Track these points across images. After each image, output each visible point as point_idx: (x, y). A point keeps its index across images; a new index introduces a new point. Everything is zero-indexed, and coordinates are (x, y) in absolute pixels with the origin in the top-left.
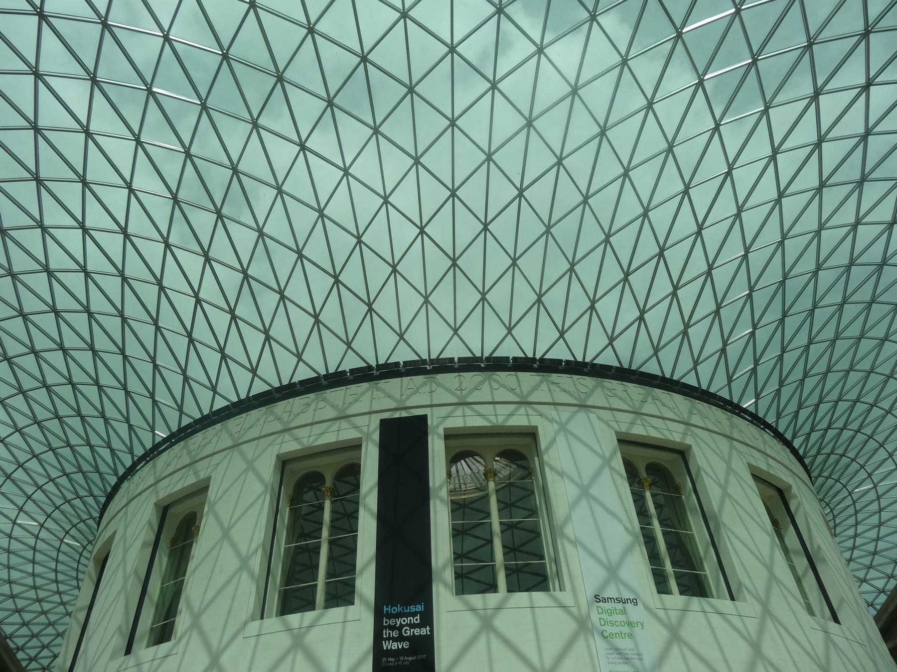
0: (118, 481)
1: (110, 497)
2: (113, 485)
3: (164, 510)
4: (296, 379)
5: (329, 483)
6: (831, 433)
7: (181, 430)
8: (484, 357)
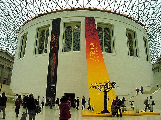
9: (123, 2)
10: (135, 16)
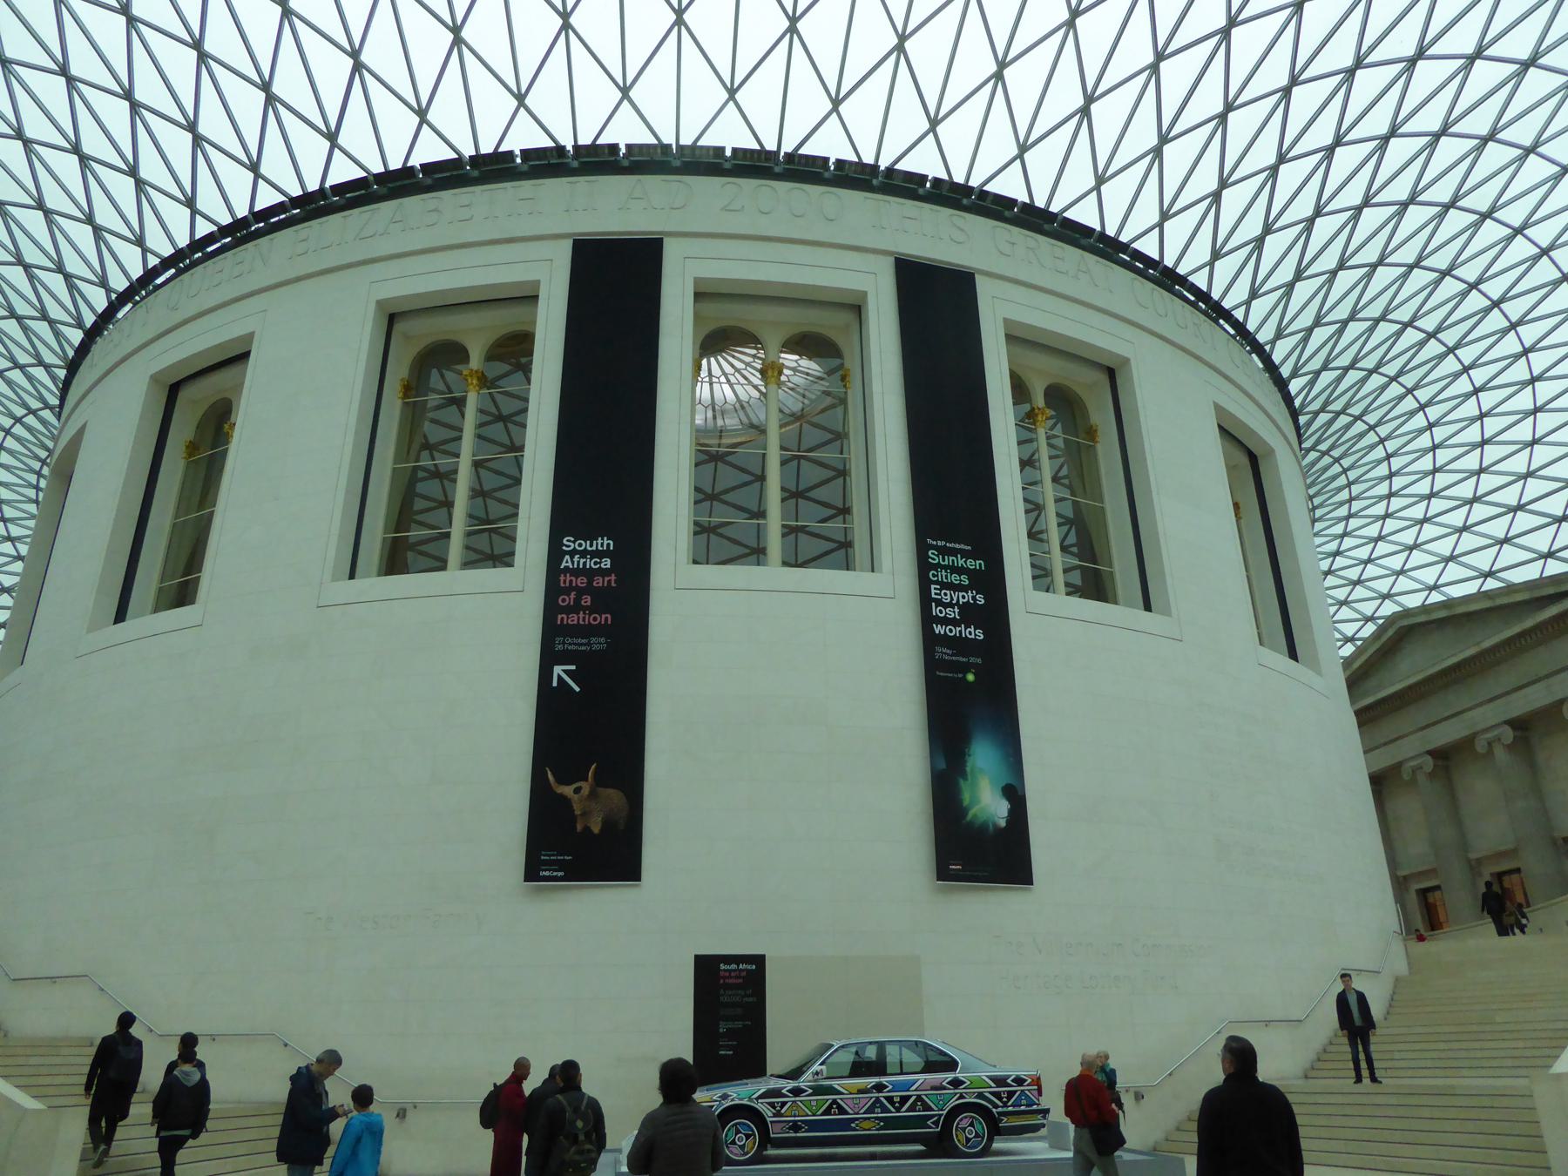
0: (85, 339)
1: (73, 367)
2: (77, 346)
3: (173, 390)
4: (416, 161)
5: (476, 361)
7: (197, 245)
8: (782, 154)
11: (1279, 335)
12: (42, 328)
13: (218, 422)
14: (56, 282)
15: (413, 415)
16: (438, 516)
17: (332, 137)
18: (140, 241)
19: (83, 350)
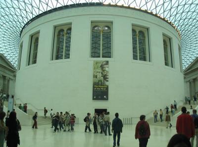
1: (21, 32)
3: (32, 36)
5: (65, 32)
6: (187, 31)
9: (161, 2)
10: (172, 20)
11: (178, 26)
12: (17, 28)
13: (37, 39)
14: (18, 23)
15: (58, 39)
16: (62, 50)
17: (47, 5)
18: (27, 18)
19: (22, 30)
